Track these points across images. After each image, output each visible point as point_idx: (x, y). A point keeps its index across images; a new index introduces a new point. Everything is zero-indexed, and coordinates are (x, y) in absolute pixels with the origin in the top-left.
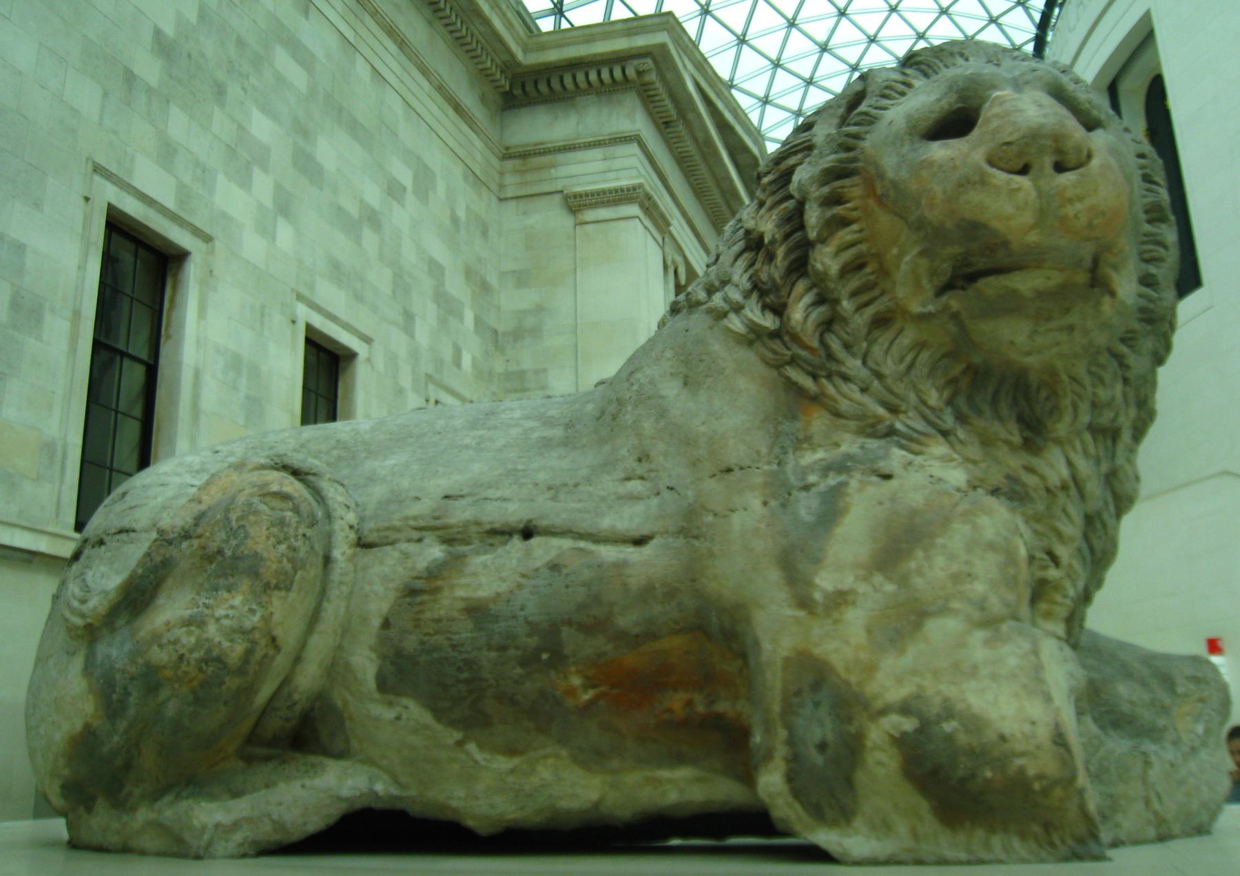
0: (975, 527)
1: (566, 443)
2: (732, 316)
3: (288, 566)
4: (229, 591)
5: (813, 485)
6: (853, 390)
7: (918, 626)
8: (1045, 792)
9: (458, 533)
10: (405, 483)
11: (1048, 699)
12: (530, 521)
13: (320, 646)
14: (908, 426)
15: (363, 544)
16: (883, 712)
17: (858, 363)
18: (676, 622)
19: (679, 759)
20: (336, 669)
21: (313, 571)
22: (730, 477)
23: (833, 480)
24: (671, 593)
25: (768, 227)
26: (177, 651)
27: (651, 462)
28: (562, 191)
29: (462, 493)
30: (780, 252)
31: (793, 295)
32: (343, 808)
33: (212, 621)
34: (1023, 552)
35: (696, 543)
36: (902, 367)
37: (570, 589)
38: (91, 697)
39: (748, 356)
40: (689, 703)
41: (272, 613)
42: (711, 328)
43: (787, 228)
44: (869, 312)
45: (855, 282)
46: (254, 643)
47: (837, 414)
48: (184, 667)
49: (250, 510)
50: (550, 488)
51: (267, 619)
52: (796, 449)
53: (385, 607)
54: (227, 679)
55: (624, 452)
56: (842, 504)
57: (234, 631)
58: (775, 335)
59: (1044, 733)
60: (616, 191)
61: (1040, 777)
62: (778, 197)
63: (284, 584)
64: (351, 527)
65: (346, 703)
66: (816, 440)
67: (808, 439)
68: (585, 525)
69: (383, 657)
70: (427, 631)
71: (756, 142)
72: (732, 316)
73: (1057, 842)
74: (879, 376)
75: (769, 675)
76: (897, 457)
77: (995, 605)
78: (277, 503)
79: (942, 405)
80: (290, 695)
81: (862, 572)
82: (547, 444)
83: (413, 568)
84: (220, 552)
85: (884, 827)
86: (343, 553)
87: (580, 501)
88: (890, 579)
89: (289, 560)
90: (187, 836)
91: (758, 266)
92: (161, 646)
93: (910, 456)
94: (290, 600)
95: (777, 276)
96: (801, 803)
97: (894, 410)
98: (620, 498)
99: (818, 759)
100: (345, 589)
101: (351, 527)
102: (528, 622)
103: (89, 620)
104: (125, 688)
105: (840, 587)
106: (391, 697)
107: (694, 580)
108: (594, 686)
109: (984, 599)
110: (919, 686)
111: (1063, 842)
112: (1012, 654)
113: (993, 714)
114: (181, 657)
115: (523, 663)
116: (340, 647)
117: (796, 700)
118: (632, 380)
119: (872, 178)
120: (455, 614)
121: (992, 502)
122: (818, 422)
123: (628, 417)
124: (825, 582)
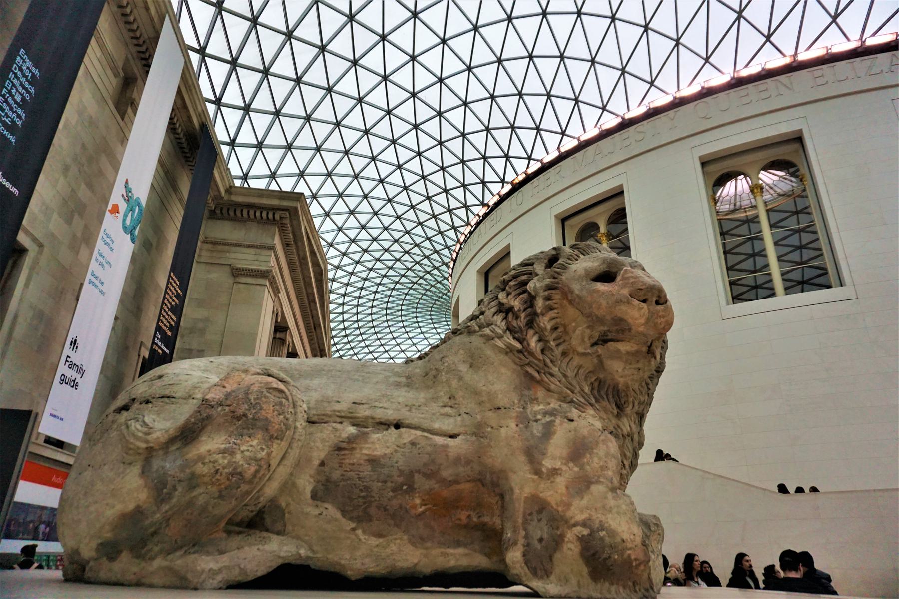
0: (607, 446)
1: (408, 385)
2: (497, 340)
3: (284, 428)
4: (250, 437)
5: (539, 420)
7: (588, 487)
9: (362, 421)
12: (399, 420)
13: (282, 472)
15: (310, 422)
16: (575, 525)
17: (557, 369)
18: (469, 476)
19: (458, 544)
20: (289, 486)
23: (548, 419)
24: (468, 462)
25: (517, 304)
26: (215, 467)
27: (456, 400)
29: (362, 402)
30: (523, 315)
32: (280, 562)
33: (239, 452)
35: (482, 440)
37: (420, 455)
38: (146, 490)
40: (469, 516)
41: (272, 451)
42: (484, 343)
43: (525, 306)
45: (554, 335)
46: (260, 466)
47: (549, 390)
48: (218, 477)
50: (406, 406)
53: (322, 455)
54: (242, 485)
55: (442, 394)
56: (553, 430)
57: (251, 458)
58: (520, 352)
59: (638, 540)
61: (636, 559)
62: (518, 291)
63: (279, 438)
64: (305, 412)
65: (288, 505)
66: (540, 400)
67: (536, 399)
68: (425, 424)
71: (323, 263)
73: (638, 590)
74: (565, 376)
75: (517, 505)
76: (574, 414)
80: (258, 498)
81: (564, 461)
82: (398, 385)
83: (340, 437)
84: (245, 415)
86: (301, 425)
87: (422, 414)
88: (576, 465)
89: (284, 424)
92: (204, 464)
93: (581, 413)
97: (573, 392)
98: (441, 415)
100: (300, 444)
101: (305, 412)
102: (400, 470)
103: (152, 445)
105: (554, 466)
106: (319, 503)
107: (480, 457)
108: (425, 505)
110: (590, 514)
111: (640, 590)
114: (217, 471)
116: (291, 474)
117: (529, 517)
119: (567, 293)
120: (362, 462)
122: (541, 393)
123: (443, 378)
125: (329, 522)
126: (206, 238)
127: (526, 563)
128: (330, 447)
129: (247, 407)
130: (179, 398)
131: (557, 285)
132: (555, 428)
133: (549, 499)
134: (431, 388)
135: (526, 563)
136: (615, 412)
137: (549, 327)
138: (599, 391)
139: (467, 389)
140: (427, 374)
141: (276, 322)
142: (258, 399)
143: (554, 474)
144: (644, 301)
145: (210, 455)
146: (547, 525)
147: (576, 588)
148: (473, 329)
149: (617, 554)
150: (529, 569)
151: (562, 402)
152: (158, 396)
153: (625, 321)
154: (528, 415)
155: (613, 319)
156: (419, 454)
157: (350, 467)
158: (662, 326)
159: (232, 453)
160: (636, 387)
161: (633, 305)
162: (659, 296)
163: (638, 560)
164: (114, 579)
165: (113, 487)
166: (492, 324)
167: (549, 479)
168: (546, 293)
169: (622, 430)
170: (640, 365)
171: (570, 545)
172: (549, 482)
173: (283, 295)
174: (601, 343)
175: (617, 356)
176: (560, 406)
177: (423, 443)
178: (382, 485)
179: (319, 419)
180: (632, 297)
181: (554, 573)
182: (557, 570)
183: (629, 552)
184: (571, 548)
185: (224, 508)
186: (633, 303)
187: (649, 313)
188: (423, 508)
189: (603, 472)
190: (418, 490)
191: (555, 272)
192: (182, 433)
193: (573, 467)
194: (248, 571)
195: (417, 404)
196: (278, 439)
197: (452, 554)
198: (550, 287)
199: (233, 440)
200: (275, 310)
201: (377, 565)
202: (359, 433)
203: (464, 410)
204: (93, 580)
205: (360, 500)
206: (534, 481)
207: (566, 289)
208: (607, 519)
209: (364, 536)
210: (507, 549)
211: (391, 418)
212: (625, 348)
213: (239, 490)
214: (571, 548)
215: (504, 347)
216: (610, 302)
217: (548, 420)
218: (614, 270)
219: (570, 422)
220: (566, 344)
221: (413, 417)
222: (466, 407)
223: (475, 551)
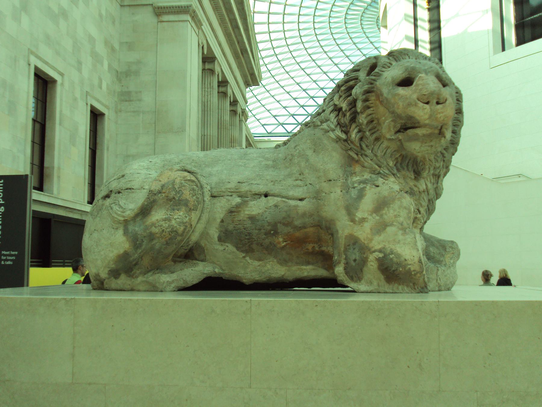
0: (401, 202)
1: (274, 167)
2: (331, 132)
4: (178, 211)
5: (356, 187)
6: (368, 159)
7: (384, 229)
8: (415, 275)
9: (244, 194)
10: (224, 177)
11: (418, 250)
12: (267, 191)
13: (200, 227)
15: (213, 196)
16: (374, 252)
19: (308, 263)
20: (205, 234)
22: (331, 183)
23: (362, 186)
24: (311, 215)
25: (344, 106)
26: (161, 228)
27: (304, 175)
28: (152, 4)
29: (244, 181)
30: (348, 114)
32: (205, 276)
33: (173, 219)
34: (413, 210)
35: (320, 201)
36: (383, 154)
37: (281, 213)
38: (128, 242)
39: (337, 146)
40: (314, 247)
41: (192, 217)
42: (323, 135)
43: (350, 107)
44: (374, 136)
45: (370, 126)
46: (186, 226)
47: (363, 167)
48: (164, 234)
49: (181, 186)
50: (272, 181)
51: (190, 219)
52: (351, 176)
53: (222, 216)
56: (364, 193)
57: (180, 223)
58: (345, 141)
59: (416, 260)
60: (179, 7)
61: (414, 271)
63: (195, 209)
64: (209, 191)
65: (206, 245)
67: (355, 173)
68: (284, 193)
69: (221, 231)
70: (236, 224)
73: (416, 288)
74: (376, 156)
75: (340, 240)
76: (380, 181)
78: (190, 183)
79: (393, 166)
80: (188, 242)
82: (267, 167)
84: (174, 198)
85: (371, 283)
86: (208, 199)
87: (282, 186)
88: (378, 215)
90: (157, 285)
91: (340, 117)
92: (155, 227)
93: (384, 181)
94: (196, 213)
95: (347, 122)
96: (347, 276)
97: (380, 167)
99: (353, 264)
101: (209, 191)
103: (126, 218)
104: (142, 240)
105: (363, 217)
106: (223, 243)
107: (318, 212)
108: (286, 241)
109: (402, 222)
110: (385, 246)
111: (418, 288)
112: (409, 238)
114: (163, 231)
115: (266, 234)
116: (205, 228)
120: (245, 219)
121: (406, 195)
122: (358, 168)
123: (296, 160)
127: (346, 273)
129: (174, 194)
130: (136, 189)
131: (373, 89)
132: (366, 192)
133: (360, 237)
134: (288, 168)
135: (346, 274)
136: (413, 177)
137: (365, 122)
138: (401, 164)
139: (311, 168)
140: (286, 158)
141: (203, 53)
143: (363, 221)
144: (427, 103)
145: (158, 222)
146: (358, 252)
147: (377, 287)
148: (316, 124)
149: (402, 268)
150: (348, 277)
151: (372, 174)
152: (124, 189)
155: (406, 116)
156: (280, 212)
157: (239, 222)
158: (442, 119)
160: (432, 157)
161: (419, 107)
162: (438, 99)
163: (416, 271)
164: (119, 288)
165: (110, 241)
166: (329, 120)
167: (360, 225)
168: (364, 97)
169: (419, 188)
170: (432, 143)
171: (372, 263)
173: (206, 27)
174: (402, 130)
175: (416, 138)
176: (370, 177)
177: (282, 205)
179: (218, 194)
181: (363, 279)
182: (366, 278)
183: (409, 266)
184: (372, 265)
185: (171, 249)
187: (431, 111)
188: (285, 243)
189: (396, 219)
190: (280, 233)
191: (372, 80)
193: (375, 217)
194: (188, 281)
195: (279, 180)
197: (305, 269)
198: (368, 92)
199: (169, 213)
200: (200, 43)
201: (260, 277)
202: (242, 202)
203: (309, 182)
204: (108, 288)
205: (246, 240)
206: (350, 225)
208: (396, 247)
209: (251, 261)
210: (335, 266)
211: (262, 191)
213: (176, 239)
214: (372, 265)
216: (405, 104)
217: (362, 187)
218: (413, 76)
221: (276, 189)
222: (310, 180)
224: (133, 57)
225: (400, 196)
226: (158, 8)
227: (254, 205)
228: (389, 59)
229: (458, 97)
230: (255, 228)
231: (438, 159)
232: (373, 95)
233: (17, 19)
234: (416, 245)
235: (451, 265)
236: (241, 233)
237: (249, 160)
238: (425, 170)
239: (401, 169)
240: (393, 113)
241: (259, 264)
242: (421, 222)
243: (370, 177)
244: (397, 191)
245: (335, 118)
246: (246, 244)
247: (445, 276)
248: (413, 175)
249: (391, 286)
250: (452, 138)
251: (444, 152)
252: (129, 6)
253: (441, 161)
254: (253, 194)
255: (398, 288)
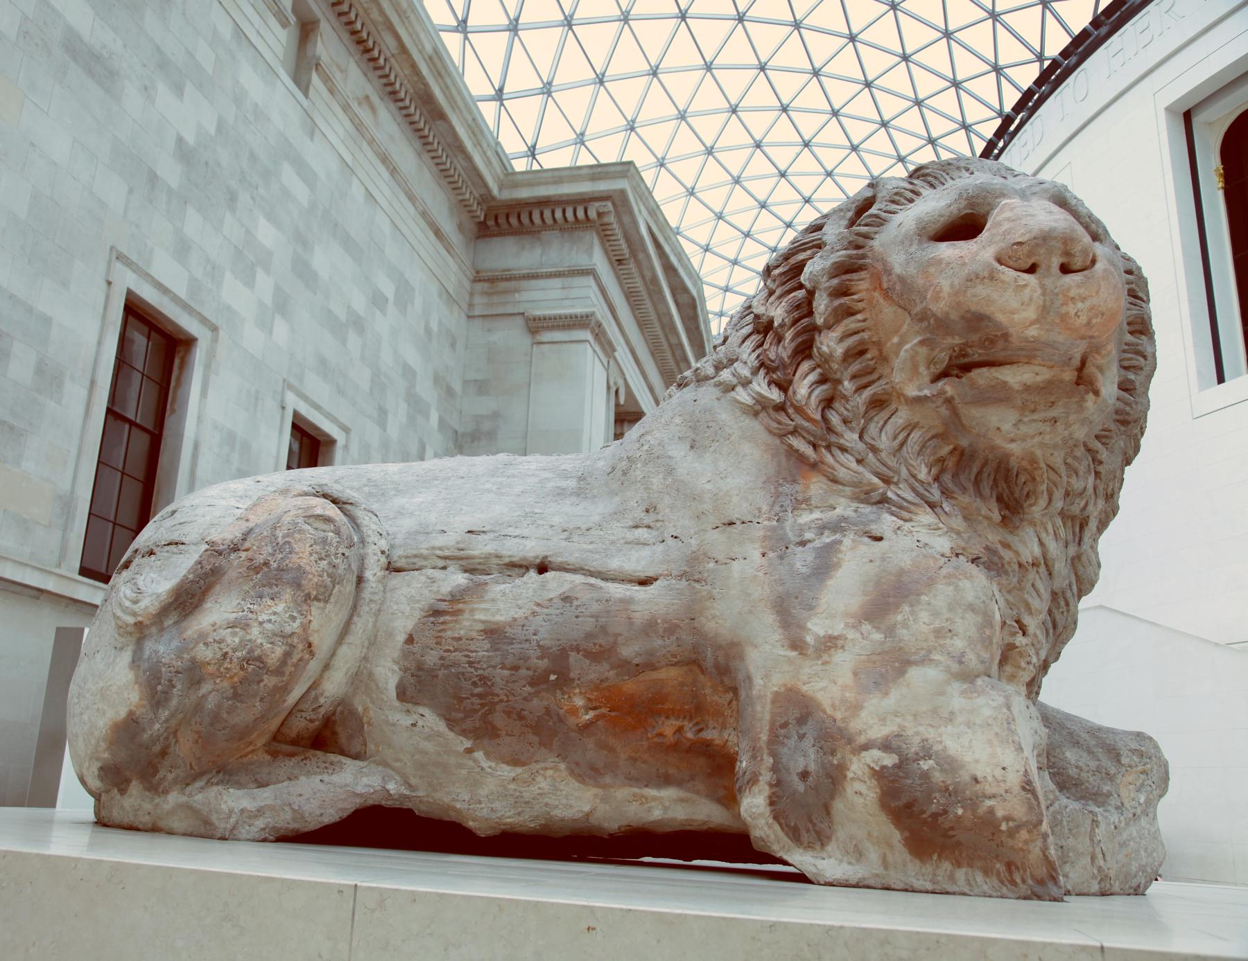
0: (957, 588)
1: (580, 493)
2: (739, 389)
5: (809, 541)
7: (901, 672)
8: (1012, 833)
9: (479, 564)
10: (432, 518)
11: (1020, 749)
12: (546, 557)
14: (898, 496)
16: (866, 747)
17: (856, 436)
18: (674, 656)
19: (666, 781)
21: (350, 587)
23: (827, 538)
24: (671, 629)
29: (484, 529)
30: (789, 335)
31: (798, 374)
35: (697, 586)
37: (580, 619)
39: (755, 426)
40: (680, 730)
42: (718, 399)
43: (796, 314)
45: (855, 367)
47: (835, 481)
53: (410, 625)
55: (633, 503)
56: (835, 559)
58: (780, 408)
59: (1014, 779)
61: (1007, 819)
64: (383, 552)
67: (806, 500)
68: (595, 564)
69: (405, 670)
72: (739, 389)
73: (1018, 880)
74: (874, 449)
75: (759, 708)
76: (886, 523)
77: (972, 660)
79: (930, 479)
81: (851, 621)
82: (561, 493)
83: (438, 592)
85: (858, 854)
87: (591, 543)
88: (878, 629)
91: (766, 346)
93: (901, 522)
97: (887, 481)
99: (801, 787)
101: (383, 552)
105: (830, 632)
108: (595, 708)
109: (963, 654)
110: (902, 728)
111: (1024, 881)
113: (968, 758)
117: (783, 731)
118: (642, 441)
120: (474, 634)
122: (816, 486)
123: (638, 472)
124: (817, 627)
125: (428, 738)
126: (478, 272)
128: (422, 610)
129: (270, 551)
131: (861, 262)
132: (840, 556)
135: (776, 818)
136: (996, 516)
137: (839, 351)
139: (678, 490)
141: (617, 405)
142: (287, 535)
143: (830, 648)
144: (1032, 270)
146: (814, 746)
147: (879, 870)
149: (962, 807)
150: (782, 829)
151: (862, 502)
153: (989, 318)
154: (785, 534)
155: (962, 317)
156: (577, 617)
158: (1083, 319)
159: (246, 627)
160: (1058, 460)
161: (1003, 282)
162: (1067, 253)
163: (1014, 820)
166: (737, 360)
167: (819, 657)
168: (835, 281)
169: (1017, 553)
171: (858, 786)
172: (820, 662)
173: (622, 353)
174: (955, 372)
175: (1000, 396)
176: (856, 511)
177: (585, 596)
178: (511, 675)
180: (1001, 264)
181: (834, 838)
182: (841, 834)
183: (989, 803)
186: (1002, 277)
187: (1044, 294)
189: (942, 642)
190: (577, 682)
192: (176, 600)
195: (584, 527)
196: (319, 600)
197: (655, 799)
198: (846, 269)
200: (612, 383)
201: (519, 814)
205: (476, 701)
206: (790, 661)
207: (880, 266)
208: (940, 735)
209: (490, 763)
212: (1019, 378)
215: (749, 401)
217: (828, 540)
218: (982, 211)
219: (876, 543)
220: (882, 382)
223: (698, 793)
224: (485, 405)
225: (951, 570)
226: (534, 320)
227: (504, 594)
228: (911, 183)
229: (1133, 286)
230: (502, 663)
231: (1076, 464)
232: (862, 277)
233: (266, 326)
234: (1013, 732)
235: (1138, 811)
236: (459, 678)
237: (514, 476)
238: (1037, 498)
239: (955, 489)
240: (923, 317)
241: (513, 775)
242: (1028, 663)
243: (856, 511)
244: (943, 555)
245: (754, 351)
246: (476, 711)
247: (1123, 845)
248: (996, 511)
249: (928, 868)
250: (1120, 405)
251: (1097, 445)
252: (483, 316)
253: (1089, 471)
254: (505, 565)
255: (952, 878)
